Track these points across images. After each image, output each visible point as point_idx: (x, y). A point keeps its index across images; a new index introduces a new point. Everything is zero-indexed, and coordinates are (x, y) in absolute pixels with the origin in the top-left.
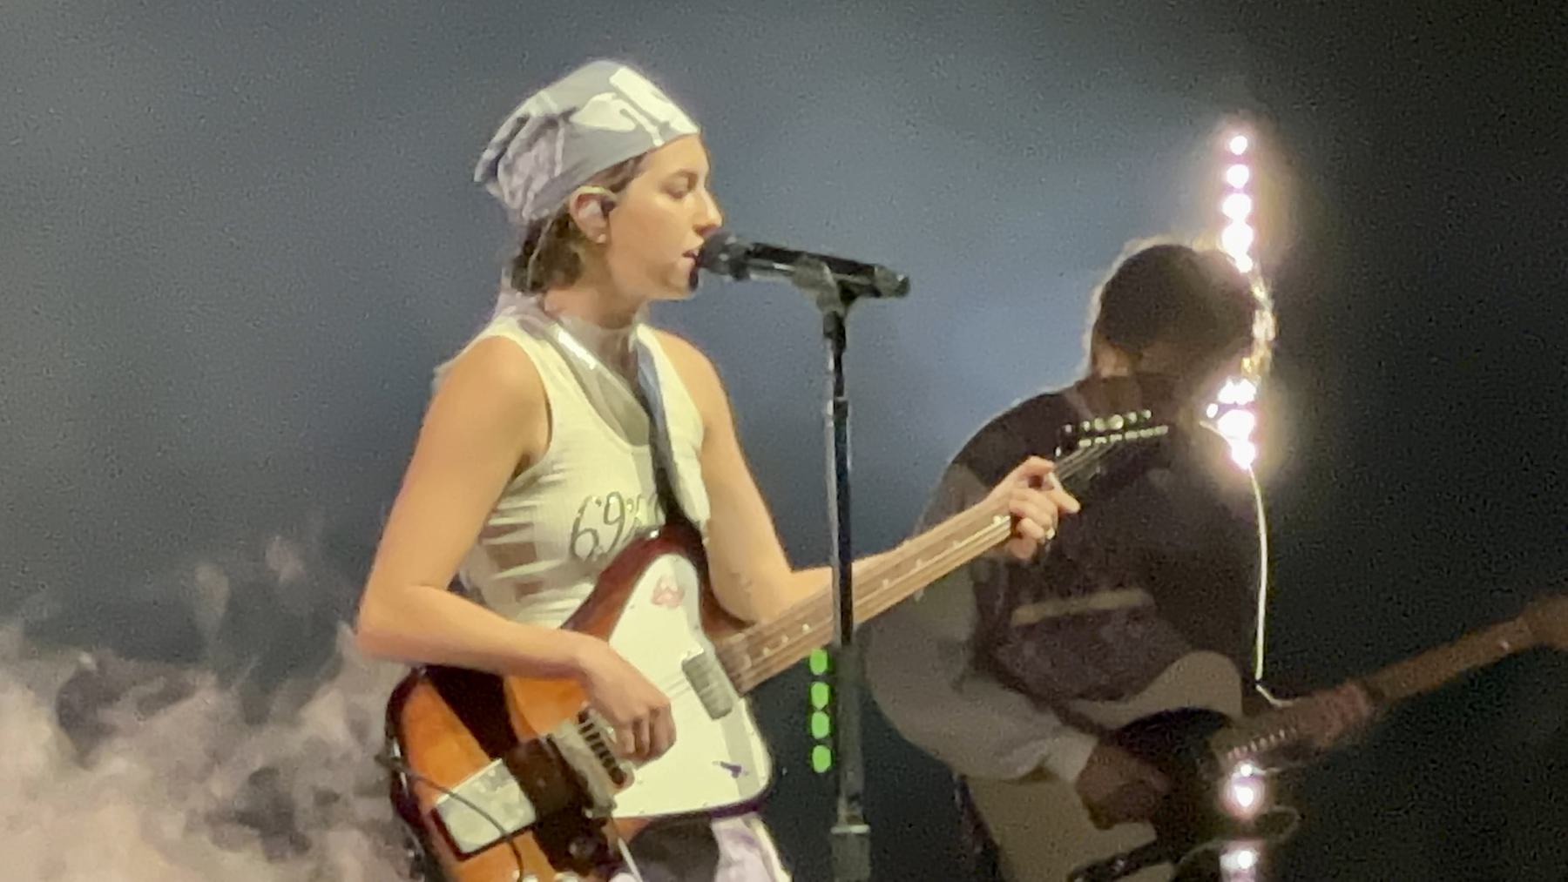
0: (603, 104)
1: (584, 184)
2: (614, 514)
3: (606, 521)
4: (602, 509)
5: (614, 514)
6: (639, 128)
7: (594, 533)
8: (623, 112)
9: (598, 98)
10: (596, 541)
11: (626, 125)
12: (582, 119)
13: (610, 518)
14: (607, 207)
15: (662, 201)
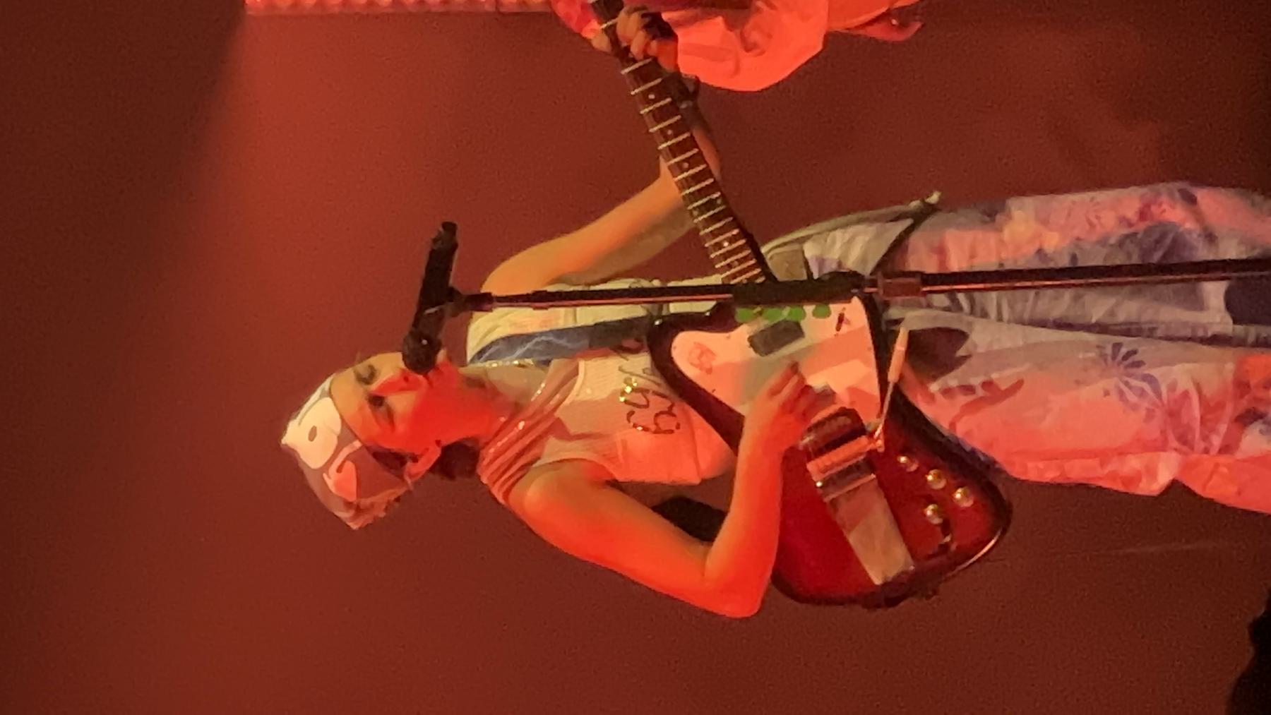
0: (338, 484)
1: (401, 477)
2: (639, 399)
3: (647, 406)
4: (636, 410)
5: (639, 399)
6: (347, 458)
7: (657, 415)
8: (339, 470)
9: (333, 489)
10: (662, 413)
11: (350, 466)
12: (353, 499)
13: (643, 402)
14: (415, 460)
15: (401, 427)
